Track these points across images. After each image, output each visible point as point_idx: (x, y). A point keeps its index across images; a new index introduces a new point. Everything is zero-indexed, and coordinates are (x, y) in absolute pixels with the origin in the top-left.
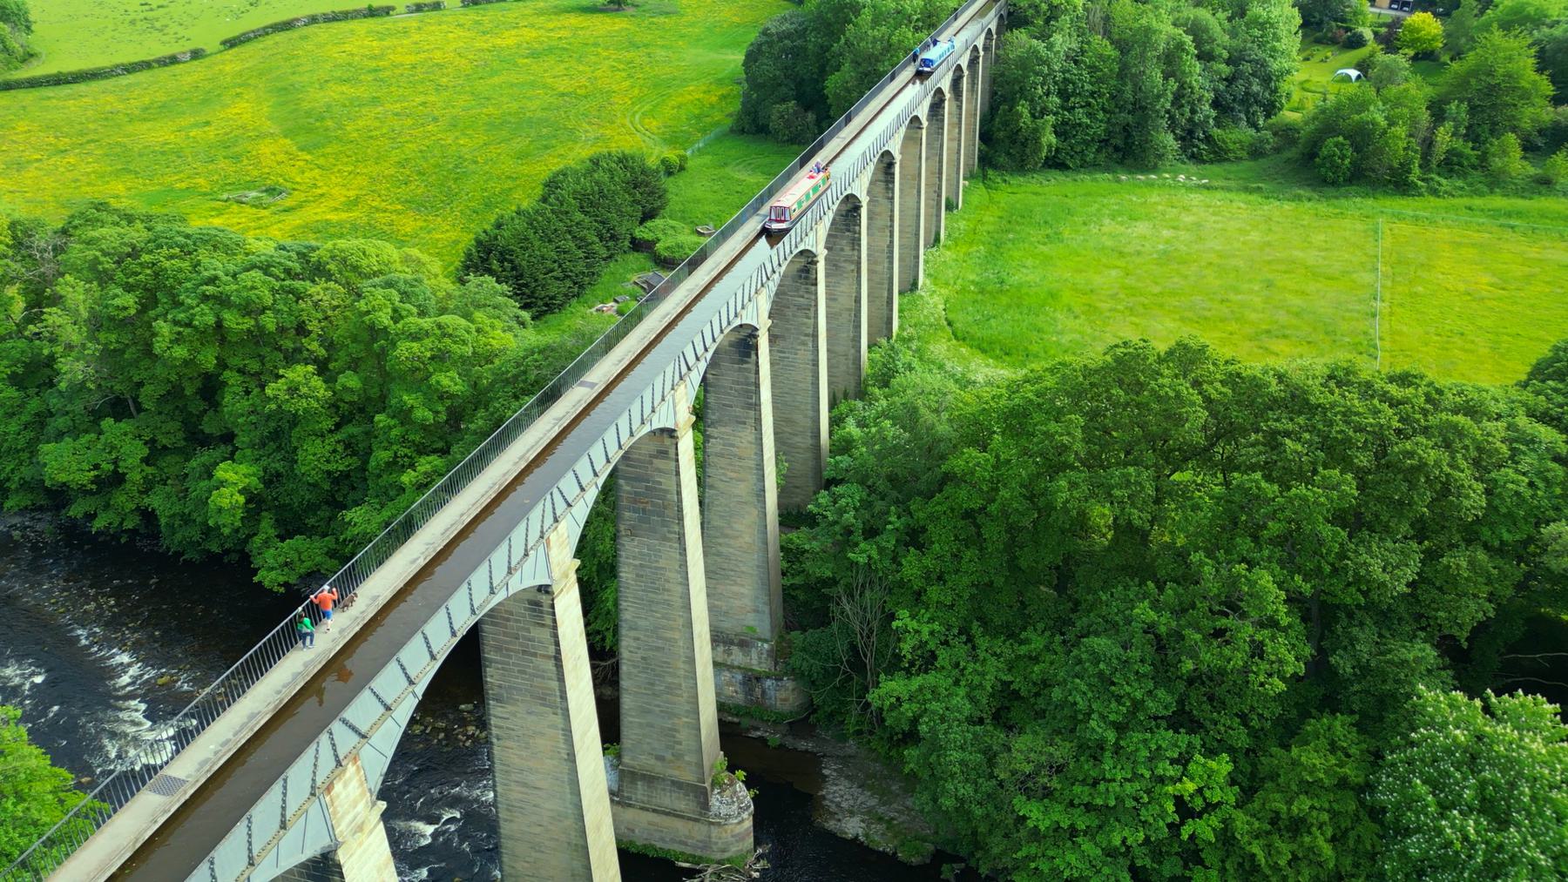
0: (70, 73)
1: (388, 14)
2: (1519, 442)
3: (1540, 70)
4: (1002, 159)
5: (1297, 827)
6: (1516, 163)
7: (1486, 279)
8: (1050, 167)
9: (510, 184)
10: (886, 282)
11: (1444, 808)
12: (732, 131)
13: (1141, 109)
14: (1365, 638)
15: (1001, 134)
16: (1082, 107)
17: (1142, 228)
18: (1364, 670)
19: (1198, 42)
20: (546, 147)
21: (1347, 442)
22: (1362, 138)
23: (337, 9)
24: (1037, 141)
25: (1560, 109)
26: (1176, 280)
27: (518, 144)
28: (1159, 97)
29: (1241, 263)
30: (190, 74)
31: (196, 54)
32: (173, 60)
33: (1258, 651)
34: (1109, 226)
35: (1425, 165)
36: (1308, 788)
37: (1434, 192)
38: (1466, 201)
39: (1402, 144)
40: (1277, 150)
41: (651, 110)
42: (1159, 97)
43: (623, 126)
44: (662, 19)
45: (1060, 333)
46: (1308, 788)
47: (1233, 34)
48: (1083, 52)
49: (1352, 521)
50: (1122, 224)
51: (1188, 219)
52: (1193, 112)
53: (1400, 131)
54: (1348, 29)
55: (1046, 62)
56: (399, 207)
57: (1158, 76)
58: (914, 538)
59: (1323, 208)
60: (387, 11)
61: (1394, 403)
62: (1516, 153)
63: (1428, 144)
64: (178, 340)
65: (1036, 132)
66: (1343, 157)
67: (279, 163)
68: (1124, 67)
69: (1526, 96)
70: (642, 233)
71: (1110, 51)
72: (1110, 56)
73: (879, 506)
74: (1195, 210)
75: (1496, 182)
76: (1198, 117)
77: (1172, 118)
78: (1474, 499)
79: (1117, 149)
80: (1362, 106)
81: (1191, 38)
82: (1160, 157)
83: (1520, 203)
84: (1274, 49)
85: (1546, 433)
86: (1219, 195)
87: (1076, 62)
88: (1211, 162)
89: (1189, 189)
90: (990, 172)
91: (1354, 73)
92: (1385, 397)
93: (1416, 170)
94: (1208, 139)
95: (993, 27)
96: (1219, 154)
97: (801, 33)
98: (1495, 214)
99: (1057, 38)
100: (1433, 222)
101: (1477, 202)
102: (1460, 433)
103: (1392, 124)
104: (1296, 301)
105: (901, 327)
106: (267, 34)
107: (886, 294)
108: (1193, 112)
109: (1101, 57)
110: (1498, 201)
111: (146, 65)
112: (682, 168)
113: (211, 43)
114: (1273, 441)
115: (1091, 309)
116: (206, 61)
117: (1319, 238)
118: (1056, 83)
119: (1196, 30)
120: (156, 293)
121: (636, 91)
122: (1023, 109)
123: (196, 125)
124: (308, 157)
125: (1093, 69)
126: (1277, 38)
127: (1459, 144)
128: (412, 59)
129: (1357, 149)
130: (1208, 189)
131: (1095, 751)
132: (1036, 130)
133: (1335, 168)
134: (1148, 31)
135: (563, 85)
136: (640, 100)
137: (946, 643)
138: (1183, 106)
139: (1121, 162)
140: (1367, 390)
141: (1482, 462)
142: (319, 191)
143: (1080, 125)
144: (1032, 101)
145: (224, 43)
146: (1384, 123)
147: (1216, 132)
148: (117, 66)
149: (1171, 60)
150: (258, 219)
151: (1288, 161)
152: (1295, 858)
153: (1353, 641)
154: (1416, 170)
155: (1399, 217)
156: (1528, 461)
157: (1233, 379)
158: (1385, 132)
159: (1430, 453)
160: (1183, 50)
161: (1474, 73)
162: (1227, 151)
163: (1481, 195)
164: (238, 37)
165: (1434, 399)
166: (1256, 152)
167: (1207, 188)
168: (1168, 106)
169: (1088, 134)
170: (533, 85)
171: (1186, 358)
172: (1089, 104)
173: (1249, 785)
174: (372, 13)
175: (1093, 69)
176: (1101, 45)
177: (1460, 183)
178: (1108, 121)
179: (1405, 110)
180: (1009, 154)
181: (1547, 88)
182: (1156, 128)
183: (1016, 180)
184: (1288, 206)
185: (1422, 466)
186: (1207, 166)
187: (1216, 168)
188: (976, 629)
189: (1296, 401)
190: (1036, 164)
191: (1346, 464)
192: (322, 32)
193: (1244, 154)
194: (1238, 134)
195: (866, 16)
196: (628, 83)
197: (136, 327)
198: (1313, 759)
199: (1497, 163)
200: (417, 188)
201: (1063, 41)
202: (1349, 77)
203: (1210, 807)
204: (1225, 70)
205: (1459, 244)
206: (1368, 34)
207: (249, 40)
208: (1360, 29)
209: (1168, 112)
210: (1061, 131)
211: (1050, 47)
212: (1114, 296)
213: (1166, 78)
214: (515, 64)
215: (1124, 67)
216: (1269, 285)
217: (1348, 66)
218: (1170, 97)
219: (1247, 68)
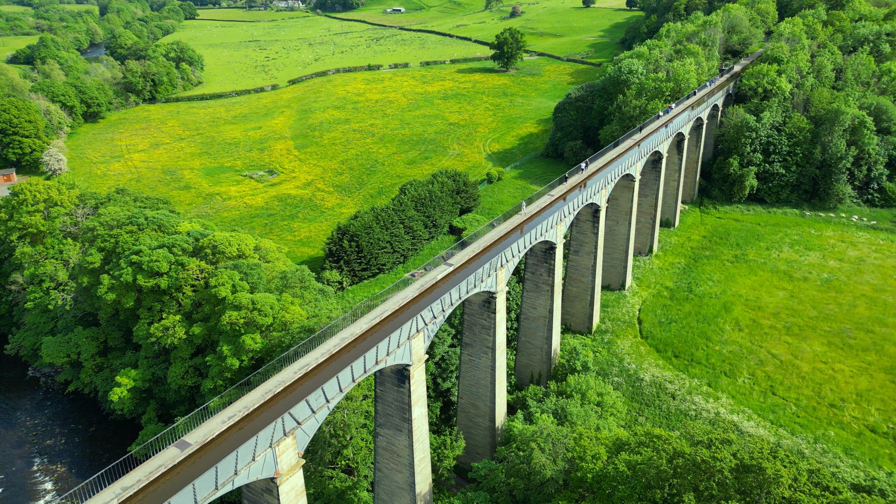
0: (209, 95)
1: (378, 69)
4: (716, 192)
8: (752, 200)
10: (590, 290)
12: (542, 155)
15: (716, 176)
16: (780, 162)
17: (814, 257)
19: (877, 120)
20: (426, 158)
24: (742, 182)
26: (831, 307)
27: (412, 155)
28: (841, 158)
30: (267, 98)
31: (274, 87)
32: (262, 90)
34: (787, 253)
41: (499, 138)
42: (841, 158)
43: (478, 147)
44: (529, 78)
45: (724, 343)
48: (785, 123)
50: (797, 252)
51: (852, 253)
52: (870, 170)
55: (756, 130)
56: (332, 189)
57: (842, 144)
60: (378, 67)
64: (111, 289)
65: (741, 179)
67: (281, 155)
70: (457, 222)
72: (804, 128)
74: (860, 246)
77: (852, 174)
81: (872, 118)
82: (840, 201)
86: (883, 235)
87: (779, 131)
88: (882, 207)
89: (859, 228)
90: (706, 201)
94: (881, 190)
95: (720, 103)
99: (766, 115)
105: (602, 320)
106: (312, 78)
107: (589, 298)
108: (870, 170)
111: (248, 92)
112: (499, 179)
113: (282, 80)
116: (278, 91)
118: (761, 144)
120: (111, 257)
121: (495, 124)
122: (735, 162)
123: (254, 129)
124: (297, 153)
125: (791, 136)
128: (378, 96)
130: (875, 229)
132: (742, 176)
134: (838, 113)
135: (453, 118)
136: (495, 130)
138: (861, 166)
142: (294, 175)
143: (777, 174)
144: (743, 155)
145: (289, 82)
147: (888, 185)
148: (233, 92)
149: (855, 133)
150: (255, 189)
160: (865, 127)
164: (297, 79)
167: (874, 228)
168: (849, 165)
169: (783, 181)
170: (436, 117)
172: (785, 160)
174: (370, 68)
175: (791, 136)
176: (800, 120)
178: (800, 173)
180: (720, 189)
182: (838, 181)
183: (727, 208)
186: (878, 209)
187: (885, 212)
190: (741, 198)
192: (339, 78)
195: (631, 92)
196: (491, 119)
200: (345, 178)
207: (302, 81)
209: (848, 169)
212: (776, 315)
214: (432, 104)
218: (851, 159)
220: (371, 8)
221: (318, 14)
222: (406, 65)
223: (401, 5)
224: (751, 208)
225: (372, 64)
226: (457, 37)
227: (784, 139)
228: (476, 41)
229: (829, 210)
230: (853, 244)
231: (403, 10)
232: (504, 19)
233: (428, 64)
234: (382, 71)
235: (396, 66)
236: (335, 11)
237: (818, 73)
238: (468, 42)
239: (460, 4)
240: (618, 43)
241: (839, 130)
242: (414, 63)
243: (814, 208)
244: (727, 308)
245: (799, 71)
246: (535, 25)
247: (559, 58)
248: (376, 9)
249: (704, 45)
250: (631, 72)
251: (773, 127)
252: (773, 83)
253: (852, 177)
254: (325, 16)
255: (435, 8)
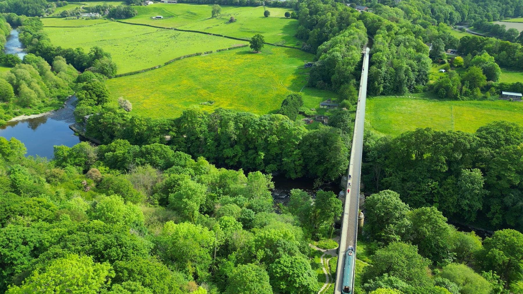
2: (474, 139)
3: (484, 74)
4: (372, 93)
5: (448, 189)
6: (480, 94)
7: (473, 117)
9: (263, 100)
11: (466, 184)
12: (306, 87)
13: (401, 82)
14: (455, 166)
17: (404, 108)
18: (455, 170)
19: (411, 68)
21: (452, 139)
22: (447, 89)
23: (190, 54)
25: (488, 82)
28: (404, 80)
29: (425, 115)
31: (160, 67)
32: (155, 68)
33: (441, 167)
34: (397, 108)
35: (461, 94)
36: (449, 184)
37: (463, 100)
38: (469, 101)
39: (456, 90)
40: (429, 90)
44: (270, 56)
45: (394, 128)
46: (449, 184)
47: (418, 66)
49: (454, 150)
51: (413, 106)
52: (411, 82)
53: (455, 87)
54: (441, 59)
55: (381, 73)
57: (404, 76)
58: (386, 158)
59: (440, 103)
60: (200, 54)
61: (458, 135)
62: (479, 92)
63: (461, 90)
65: (379, 88)
66: (444, 93)
68: (397, 73)
69: (481, 79)
71: (393, 70)
73: (380, 154)
75: (475, 97)
76: (412, 83)
78: (468, 146)
79: (395, 90)
80: (447, 82)
82: (405, 92)
83: (480, 102)
84: (427, 69)
85: (478, 138)
86: (418, 100)
89: (412, 99)
90: (369, 96)
91: (444, 71)
92: (456, 134)
93: (459, 95)
94: (414, 88)
96: (416, 91)
97: (324, 66)
98: (475, 104)
99: (383, 68)
100: (463, 106)
101: (472, 102)
102: (466, 138)
103: (453, 85)
104: (437, 122)
109: (391, 72)
110: (476, 102)
114: (442, 140)
115: (399, 124)
117: (440, 110)
119: (411, 65)
122: (376, 83)
125: (390, 74)
126: (428, 66)
127: (467, 90)
129: (446, 91)
131: (419, 183)
132: (379, 87)
133: (442, 95)
134: (402, 67)
137: (394, 173)
139: (396, 93)
140: (454, 133)
141: (469, 142)
145: (165, 63)
146: (452, 86)
147: (416, 86)
149: (406, 72)
151: (432, 92)
152: (448, 193)
153: (454, 166)
154: (459, 95)
155: (456, 105)
156: (476, 141)
157: (435, 132)
158: (452, 88)
159: (462, 140)
161: (470, 74)
162: (418, 91)
163: (472, 100)
165: (463, 134)
166: (424, 91)
167: (415, 99)
171: (428, 129)
173: (441, 185)
177: (468, 98)
179: (456, 83)
181: (485, 78)
183: (375, 98)
184: (433, 103)
185: (462, 142)
187: (416, 94)
188: (398, 170)
189: (444, 135)
191: (452, 143)
192: (187, 59)
193: (422, 91)
194: (420, 87)
197: (245, 130)
198: (449, 181)
199: (476, 93)
201: (384, 69)
202: (442, 72)
203: (436, 188)
204: (417, 73)
205: (468, 111)
206: (446, 61)
207: (171, 62)
208: (444, 60)
210: (384, 87)
211: (382, 70)
213: (406, 76)
215: (397, 73)
216: (432, 119)
217: (442, 69)
219: (422, 73)
220: (140, 16)
221: (112, 20)
222: (211, 52)
223: (159, 14)
224: (382, 97)
225: (198, 52)
226: (213, 35)
227: (389, 76)
228: (225, 37)
229: (402, 95)
230: (412, 104)
231: (162, 17)
232: (227, 23)
233: (220, 51)
234: (202, 56)
235: (207, 53)
236: (121, 18)
237: (392, 53)
238: (222, 37)
239: (195, 14)
240: (294, 36)
241: (403, 72)
242: (214, 50)
243: (398, 95)
244: (391, 122)
245: (388, 54)
246: (248, 28)
247: (273, 45)
248: (146, 17)
249: (356, 46)
250: (337, 57)
251: (386, 72)
252: (382, 58)
253: (407, 85)
254: (117, 21)
255: (180, 16)
